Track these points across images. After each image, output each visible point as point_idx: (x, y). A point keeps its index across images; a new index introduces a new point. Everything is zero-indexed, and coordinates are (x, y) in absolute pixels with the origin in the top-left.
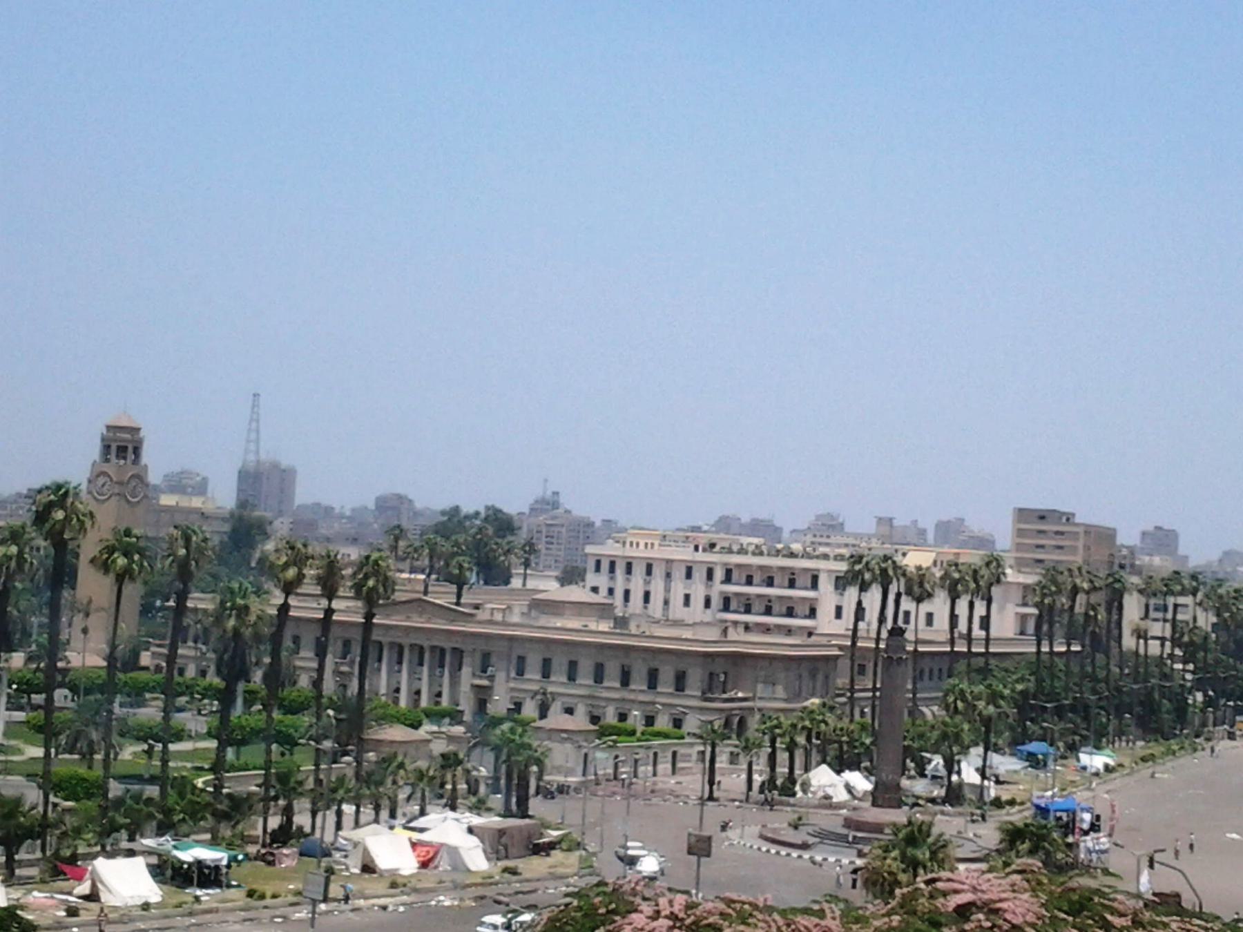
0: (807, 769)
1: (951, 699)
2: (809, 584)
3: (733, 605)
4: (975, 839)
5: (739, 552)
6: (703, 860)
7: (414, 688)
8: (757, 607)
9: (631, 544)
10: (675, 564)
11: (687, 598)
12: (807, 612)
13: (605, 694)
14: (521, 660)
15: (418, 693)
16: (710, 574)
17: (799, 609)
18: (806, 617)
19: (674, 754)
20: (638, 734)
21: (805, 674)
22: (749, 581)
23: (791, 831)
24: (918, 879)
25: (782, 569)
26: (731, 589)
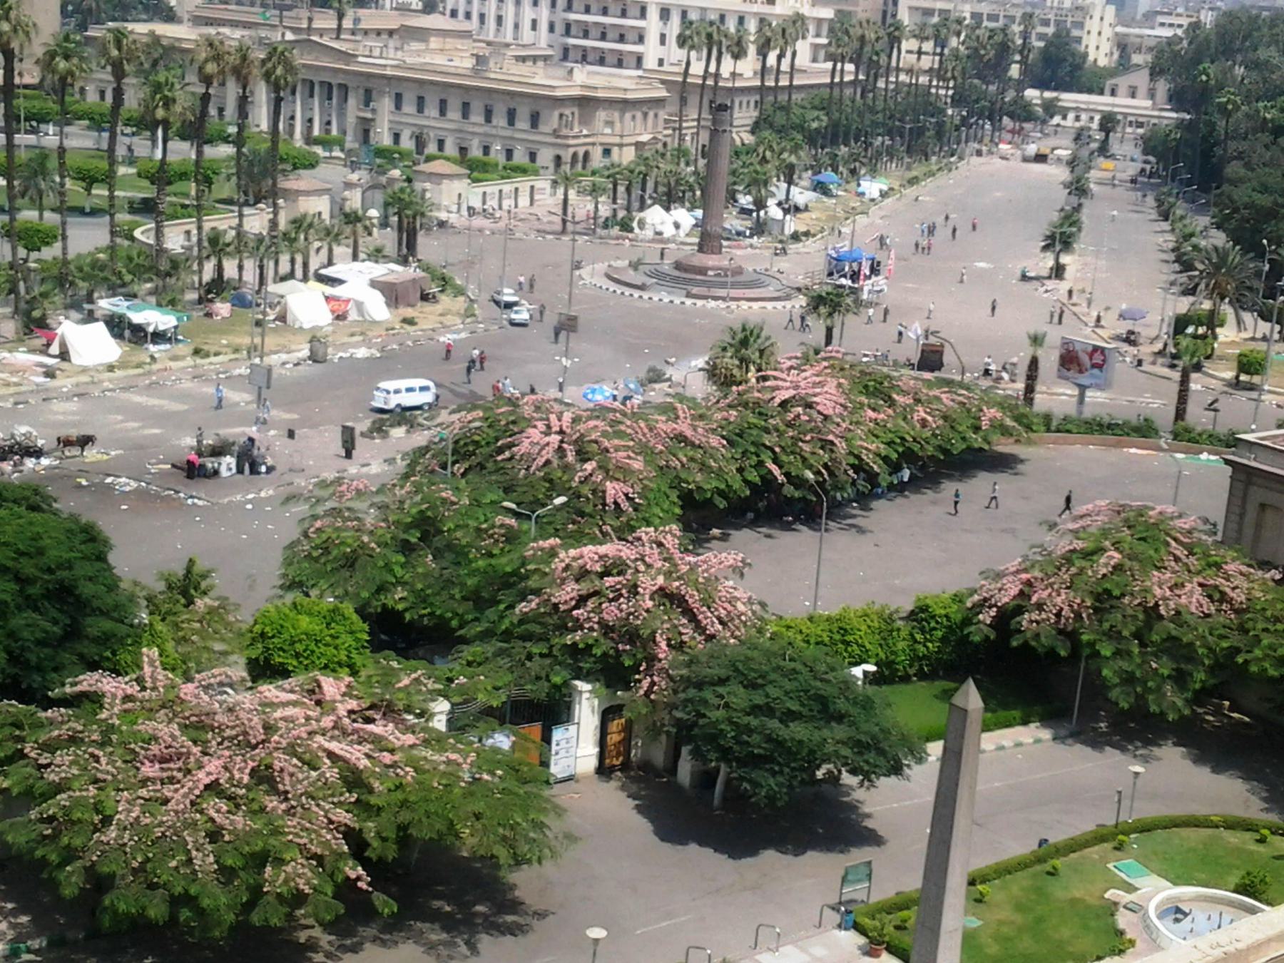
0: (642, 207)
1: (761, 150)
19: (532, 187)
20: (500, 167)
21: (639, 115)
23: (631, 272)
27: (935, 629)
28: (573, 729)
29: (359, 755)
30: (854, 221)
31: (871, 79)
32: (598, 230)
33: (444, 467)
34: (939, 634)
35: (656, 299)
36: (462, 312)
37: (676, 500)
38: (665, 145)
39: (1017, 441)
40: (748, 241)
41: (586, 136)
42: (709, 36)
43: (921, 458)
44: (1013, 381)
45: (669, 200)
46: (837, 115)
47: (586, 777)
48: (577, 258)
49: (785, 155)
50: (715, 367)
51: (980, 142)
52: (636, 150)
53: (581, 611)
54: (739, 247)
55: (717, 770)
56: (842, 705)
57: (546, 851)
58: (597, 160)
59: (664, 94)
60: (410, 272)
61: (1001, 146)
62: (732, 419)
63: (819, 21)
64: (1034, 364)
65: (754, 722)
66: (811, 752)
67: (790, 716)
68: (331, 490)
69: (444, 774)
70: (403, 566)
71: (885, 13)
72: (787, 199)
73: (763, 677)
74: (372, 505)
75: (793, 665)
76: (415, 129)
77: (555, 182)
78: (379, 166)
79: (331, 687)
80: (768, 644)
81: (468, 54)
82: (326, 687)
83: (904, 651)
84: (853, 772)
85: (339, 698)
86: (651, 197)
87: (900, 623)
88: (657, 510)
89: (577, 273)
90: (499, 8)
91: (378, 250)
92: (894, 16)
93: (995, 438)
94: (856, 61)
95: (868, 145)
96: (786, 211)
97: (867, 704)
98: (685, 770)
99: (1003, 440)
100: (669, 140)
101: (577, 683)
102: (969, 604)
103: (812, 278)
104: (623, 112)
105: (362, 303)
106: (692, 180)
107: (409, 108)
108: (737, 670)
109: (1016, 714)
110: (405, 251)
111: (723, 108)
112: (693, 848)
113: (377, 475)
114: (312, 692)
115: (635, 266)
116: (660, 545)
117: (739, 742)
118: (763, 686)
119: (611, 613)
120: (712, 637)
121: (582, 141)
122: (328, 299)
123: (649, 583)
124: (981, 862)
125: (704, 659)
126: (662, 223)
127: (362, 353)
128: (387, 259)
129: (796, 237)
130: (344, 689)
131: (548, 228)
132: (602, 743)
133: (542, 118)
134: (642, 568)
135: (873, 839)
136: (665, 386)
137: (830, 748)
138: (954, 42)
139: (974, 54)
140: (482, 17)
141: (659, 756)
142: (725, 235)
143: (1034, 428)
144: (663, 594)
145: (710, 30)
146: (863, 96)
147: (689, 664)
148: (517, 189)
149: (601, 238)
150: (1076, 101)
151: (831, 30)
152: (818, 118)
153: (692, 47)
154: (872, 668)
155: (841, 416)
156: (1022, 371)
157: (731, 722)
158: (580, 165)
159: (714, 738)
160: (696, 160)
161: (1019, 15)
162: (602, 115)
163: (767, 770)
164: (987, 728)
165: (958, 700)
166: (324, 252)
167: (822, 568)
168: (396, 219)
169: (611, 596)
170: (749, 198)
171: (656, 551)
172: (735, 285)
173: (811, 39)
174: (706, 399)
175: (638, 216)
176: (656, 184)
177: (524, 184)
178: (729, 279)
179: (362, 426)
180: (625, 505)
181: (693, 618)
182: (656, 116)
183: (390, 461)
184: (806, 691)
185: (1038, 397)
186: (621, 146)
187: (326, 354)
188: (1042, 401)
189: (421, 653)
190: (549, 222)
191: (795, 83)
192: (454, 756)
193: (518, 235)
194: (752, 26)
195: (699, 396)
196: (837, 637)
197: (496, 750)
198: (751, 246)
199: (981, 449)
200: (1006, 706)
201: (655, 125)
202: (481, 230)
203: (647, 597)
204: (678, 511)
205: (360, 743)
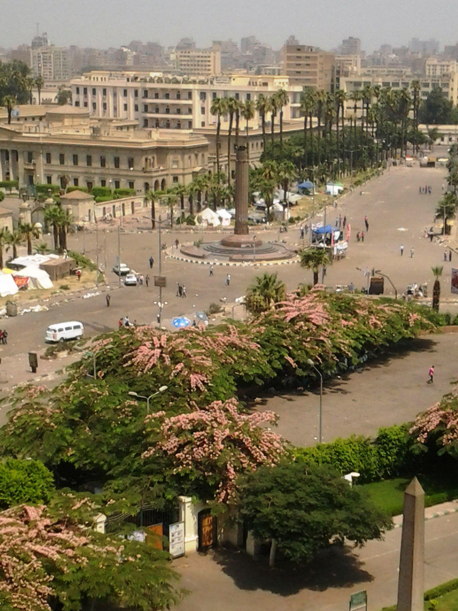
1: (267, 171)
3: (149, 109)
4: (284, 245)
5: (150, 82)
11: (126, 105)
17: (183, 110)
18: (186, 114)
19: (133, 203)
21: (193, 156)
22: (157, 96)
23: (196, 248)
24: (271, 304)
25: (173, 90)
26: (148, 101)
27: (391, 448)
28: (181, 525)
29: (53, 552)
30: (325, 209)
31: (328, 125)
32: (174, 225)
33: (92, 373)
34: (395, 451)
35: (211, 263)
36: (96, 279)
37: (233, 382)
38: (210, 172)
39: (431, 332)
40: (264, 225)
41: (162, 170)
42: (231, 107)
43: (375, 347)
44: (426, 297)
45: (215, 205)
46: (310, 147)
47: (191, 554)
48: (162, 243)
49: (282, 173)
50: (250, 301)
51: (395, 158)
52: (193, 176)
53: (181, 454)
54: (258, 229)
55: (270, 543)
56: (341, 498)
57: (172, 601)
58: (170, 184)
59: (206, 142)
60: (64, 258)
61: (407, 159)
62: (262, 332)
63: (295, 94)
64: (437, 286)
65: (289, 513)
66: (325, 528)
67: (310, 508)
68: (25, 392)
69: (106, 559)
70: (71, 435)
71: (332, 86)
72: (285, 199)
73: (293, 485)
74: (50, 400)
75: (309, 477)
76: (60, 174)
77: (146, 200)
78: (40, 197)
79: (33, 512)
80: (294, 465)
81: (88, 127)
82: (30, 513)
83: (375, 463)
84: (350, 538)
85: (38, 518)
86: (204, 204)
87: (372, 446)
88: (221, 389)
89: (163, 251)
90: (104, 99)
91: (43, 247)
92: (338, 88)
93: (418, 331)
94: (319, 116)
95: (330, 163)
96: (285, 206)
97: (356, 497)
98: (251, 545)
99: (423, 332)
100: (212, 169)
101: (183, 498)
102: (411, 432)
103: (303, 245)
104: (183, 154)
105: (36, 279)
106: (228, 192)
107: (55, 161)
108: (277, 482)
109: (444, 495)
110: (59, 246)
111: (242, 148)
112: (259, 591)
113: (52, 381)
114: (22, 516)
115: (198, 245)
116: (226, 410)
117: (282, 526)
118: (293, 491)
119: (199, 453)
120: (260, 464)
121: (160, 173)
122: (15, 278)
123: (221, 434)
124: (430, 586)
125: (257, 478)
126: (212, 218)
127: (38, 309)
128: (49, 252)
129: (292, 221)
130: (41, 513)
131: (144, 226)
132: (200, 532)
133: (136, 160)
134: (215, 425)
135: (366, 577)
136: (221, 314)
137: (336, 525)
138: (375, 100)
139: (388, 108)
140: (94, 105)
141: (234, 537)
142: (250, 222)
143: (441, 323)
144: (229, 439)
145: (230, 103)
146: (324, 135)
147: (248, 481)
148: (123, 205)
149: (176, 229)
150: (447, 130)
151: (302, 99)
152: (299, 150)
153: (220, 114)
154: (357, 475)
155: (327, 325)
156: (430, 290)
157: (275, 513)
158: (160, 188)
159: (266, 524)
160: (229, 180)
161: (410, 82)
162: (170, 157)
163: (300, 541)
164: (428, 505)
165: (409, 491)
166: (11, 251)
167: (323, 416)
168: (52, 227)
169: (198, 443)
170: (262, 200)
171: (224, 414)
172: (258, 252)
173: (290, 104)
174: (246, 321)
175: (197, 215)
176: (206, 194)
177: (127, 201)
178: (255, 249)
179: (41, 352)
180: (203, 388)
181: (246, 450)
182: (203, 155)
183: (60, 372)
184: (319, 492)
185: (441, 305)
186: (184, 175)
187: (16, 311)
188: (443, 308)
189: (86, 487)
190: (144, 223)
191: (283, 131)
192: (111, 548)
193: (126, 231)
194: (255, 98)
195: (242, 319)
196: (335, 457)
197: (136, 543)
198: (266, 228)
199: (410, 338)
200: (437, 490)
201: (203, 162)
202: (104, 230)
203: (220, 442)
204: (234, 388)
205: (53, 545)
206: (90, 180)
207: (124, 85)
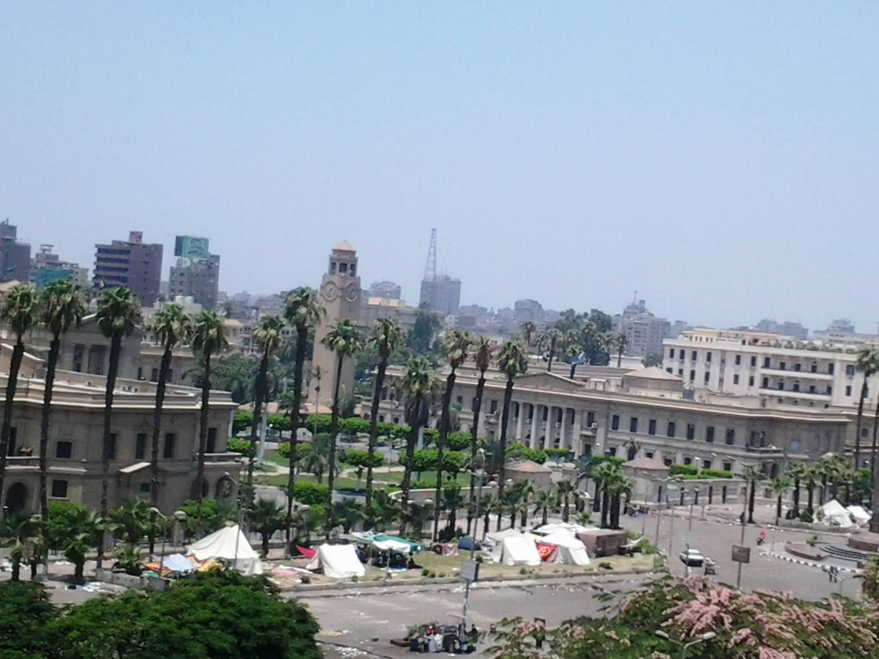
2: (827, 369)
3: (770, 384)
6: (743, 564)
7: (541, 435)
8: (788, 385)
9: (696, 338)
10: (728, 354)
11: (736, 378)
12: (825, 390)
13: (675, 444)
14: (616, 418)
15: (543, 439)
16: (754, 361)
17: (819, 388)
18: (824, 394)
19: (725, 489)
20: (699, 474)
21: (823, 436)
22: (783, 367)
23: (808, 547)
25: (807, 359)
26: (769, 372)
206: (668, 458)
207: (739, 350)
